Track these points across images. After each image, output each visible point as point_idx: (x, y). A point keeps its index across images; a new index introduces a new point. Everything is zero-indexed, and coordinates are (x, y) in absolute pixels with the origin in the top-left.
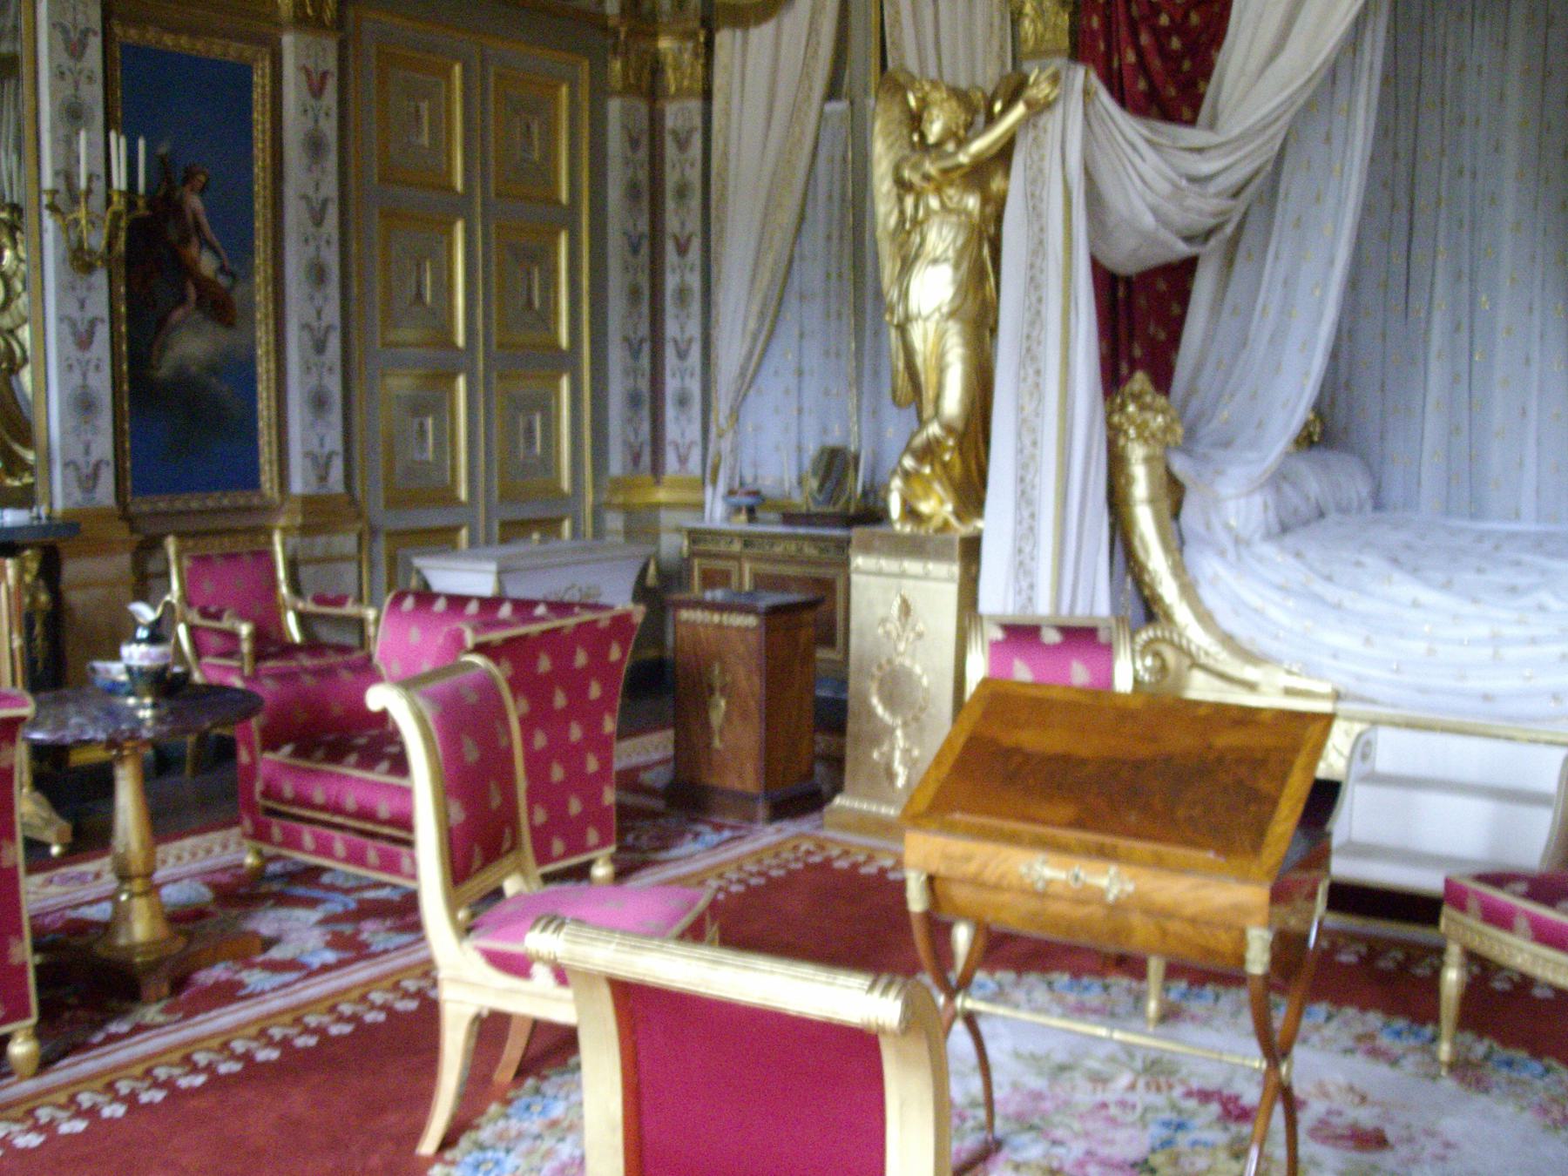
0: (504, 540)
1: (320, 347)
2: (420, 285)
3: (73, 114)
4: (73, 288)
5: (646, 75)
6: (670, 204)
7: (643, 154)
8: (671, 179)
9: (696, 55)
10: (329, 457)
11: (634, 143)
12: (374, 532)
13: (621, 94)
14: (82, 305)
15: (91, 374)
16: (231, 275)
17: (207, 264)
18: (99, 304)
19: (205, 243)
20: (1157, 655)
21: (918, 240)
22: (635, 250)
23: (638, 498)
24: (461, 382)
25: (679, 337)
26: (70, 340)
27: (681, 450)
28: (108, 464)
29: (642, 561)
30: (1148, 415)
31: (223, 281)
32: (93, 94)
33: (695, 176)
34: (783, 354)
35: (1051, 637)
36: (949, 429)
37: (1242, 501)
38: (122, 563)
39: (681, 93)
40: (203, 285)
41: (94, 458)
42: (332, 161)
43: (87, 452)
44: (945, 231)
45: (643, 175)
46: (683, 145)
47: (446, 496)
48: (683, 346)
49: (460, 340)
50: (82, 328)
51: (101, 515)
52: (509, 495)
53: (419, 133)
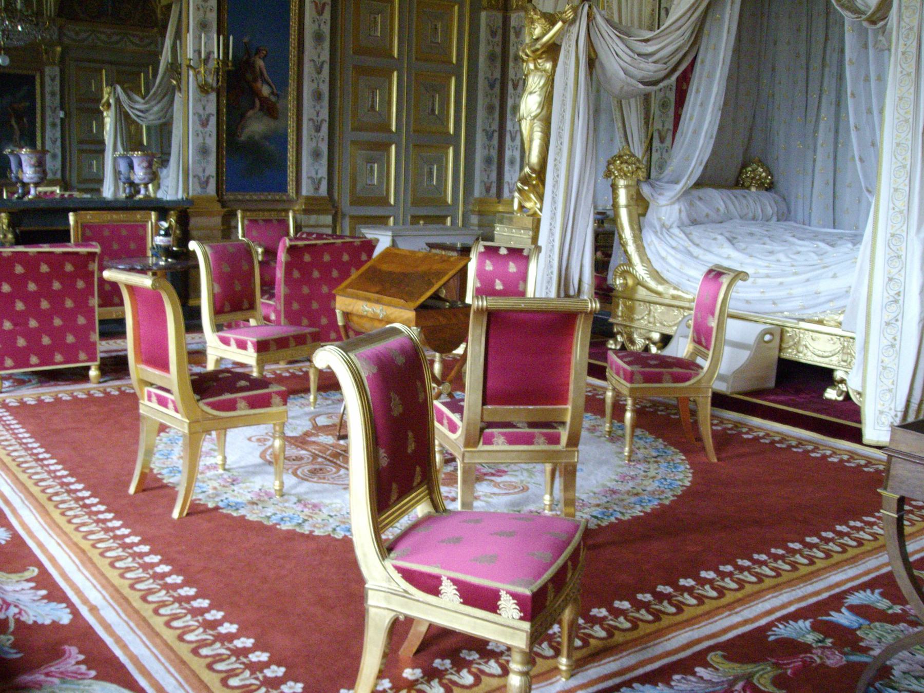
1: (318, 129)
2: (373, 101)
3: (203, 26)
4: (200, 101)
7: (499, 38)
10: (320, 180)
11: (493, 34)
13: (485, 9)
14: (204, 109)
15: (207, 138)
16: (278, 96)
17: (265, 91)
18: (212, 108)
19: (265, 81)
20: (625, 279)
22: (492, 86)
24: (393, 147)
26: (198, 122)
28: (213, 177)
31: (273, 99)
32: (213, 17)
35: (503, 251)
37: (669, 208)
38: (217, 220)
40: (264, 101)
42: (327, 44)
43: (204, 171)
44: (536, 79)
45: (498, 50)
47: (384, 201)
49: (394, 129)
50: (204, 117)
51: (209, 200)
52: (416, 203)
53: (376, 30)
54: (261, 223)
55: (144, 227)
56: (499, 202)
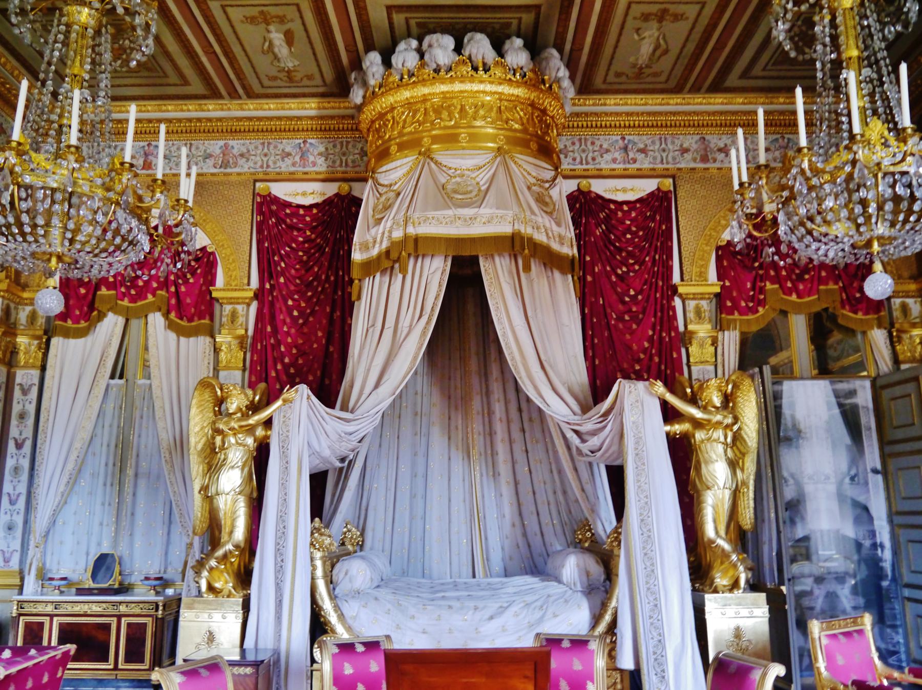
5: (8, 355)
6: (14, 422)
8: (16, 409)
9: (40, 348)
21: (223, 457)
25: (11, 492)
30: (324, 538)
33: (32, 409)
34: (76, 502)
36: (237, 547)
39: (26, 366)
44: (238, 453)
46: (25, 392)
48: (13, 498)
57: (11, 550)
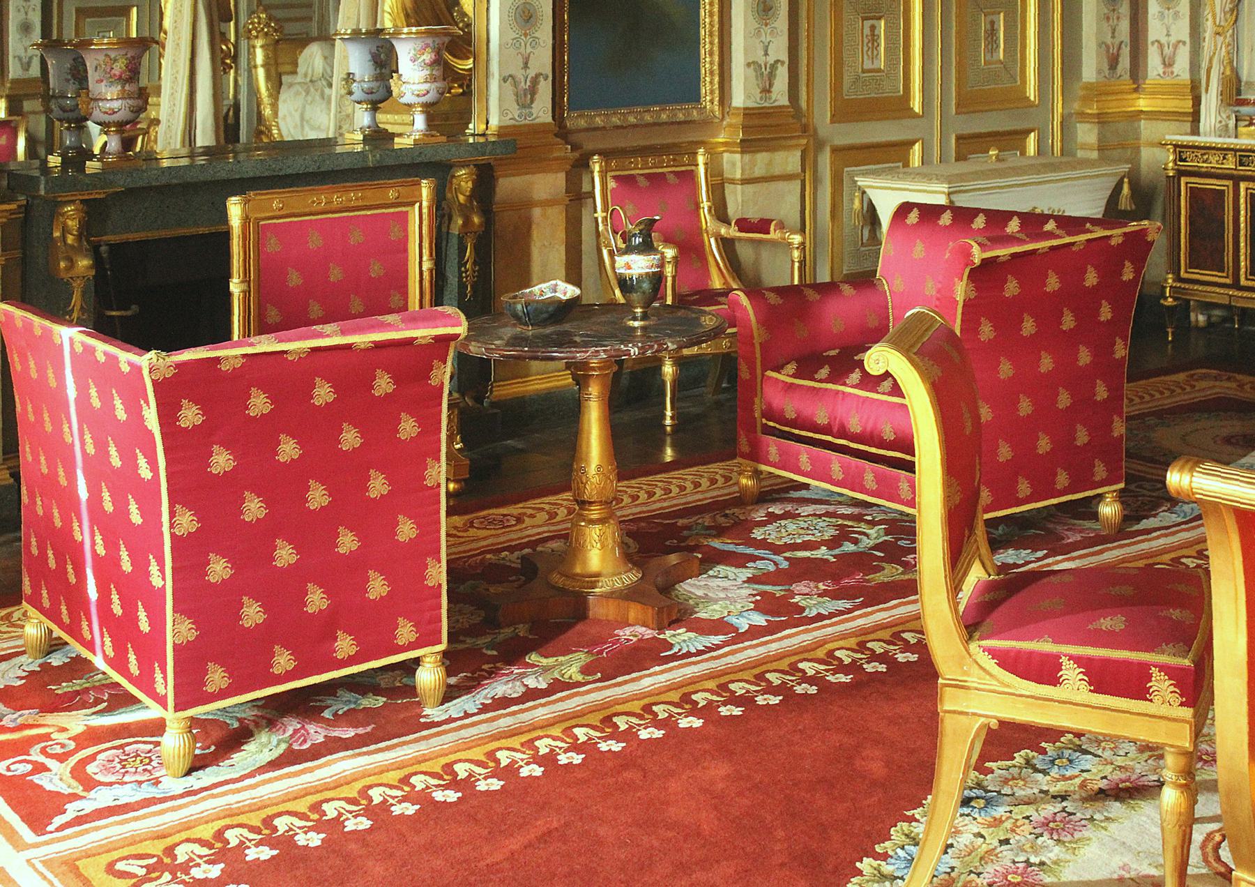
0: (960, 157)
10: (774, 66)
12: (819, 145)
23: (1113, 107)
27: (1166, 51)
28: (546, 78)
29: (1116, 179)
41: (532, 73)
47: (900, 108)
52: (967, 104)
54: (643, 182)
55: (403, 219)
56: (1136, 90)
57: (1173, 40)
